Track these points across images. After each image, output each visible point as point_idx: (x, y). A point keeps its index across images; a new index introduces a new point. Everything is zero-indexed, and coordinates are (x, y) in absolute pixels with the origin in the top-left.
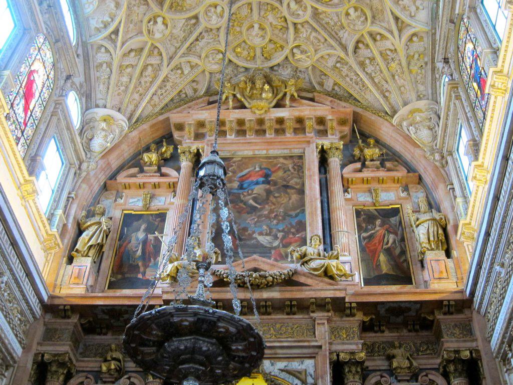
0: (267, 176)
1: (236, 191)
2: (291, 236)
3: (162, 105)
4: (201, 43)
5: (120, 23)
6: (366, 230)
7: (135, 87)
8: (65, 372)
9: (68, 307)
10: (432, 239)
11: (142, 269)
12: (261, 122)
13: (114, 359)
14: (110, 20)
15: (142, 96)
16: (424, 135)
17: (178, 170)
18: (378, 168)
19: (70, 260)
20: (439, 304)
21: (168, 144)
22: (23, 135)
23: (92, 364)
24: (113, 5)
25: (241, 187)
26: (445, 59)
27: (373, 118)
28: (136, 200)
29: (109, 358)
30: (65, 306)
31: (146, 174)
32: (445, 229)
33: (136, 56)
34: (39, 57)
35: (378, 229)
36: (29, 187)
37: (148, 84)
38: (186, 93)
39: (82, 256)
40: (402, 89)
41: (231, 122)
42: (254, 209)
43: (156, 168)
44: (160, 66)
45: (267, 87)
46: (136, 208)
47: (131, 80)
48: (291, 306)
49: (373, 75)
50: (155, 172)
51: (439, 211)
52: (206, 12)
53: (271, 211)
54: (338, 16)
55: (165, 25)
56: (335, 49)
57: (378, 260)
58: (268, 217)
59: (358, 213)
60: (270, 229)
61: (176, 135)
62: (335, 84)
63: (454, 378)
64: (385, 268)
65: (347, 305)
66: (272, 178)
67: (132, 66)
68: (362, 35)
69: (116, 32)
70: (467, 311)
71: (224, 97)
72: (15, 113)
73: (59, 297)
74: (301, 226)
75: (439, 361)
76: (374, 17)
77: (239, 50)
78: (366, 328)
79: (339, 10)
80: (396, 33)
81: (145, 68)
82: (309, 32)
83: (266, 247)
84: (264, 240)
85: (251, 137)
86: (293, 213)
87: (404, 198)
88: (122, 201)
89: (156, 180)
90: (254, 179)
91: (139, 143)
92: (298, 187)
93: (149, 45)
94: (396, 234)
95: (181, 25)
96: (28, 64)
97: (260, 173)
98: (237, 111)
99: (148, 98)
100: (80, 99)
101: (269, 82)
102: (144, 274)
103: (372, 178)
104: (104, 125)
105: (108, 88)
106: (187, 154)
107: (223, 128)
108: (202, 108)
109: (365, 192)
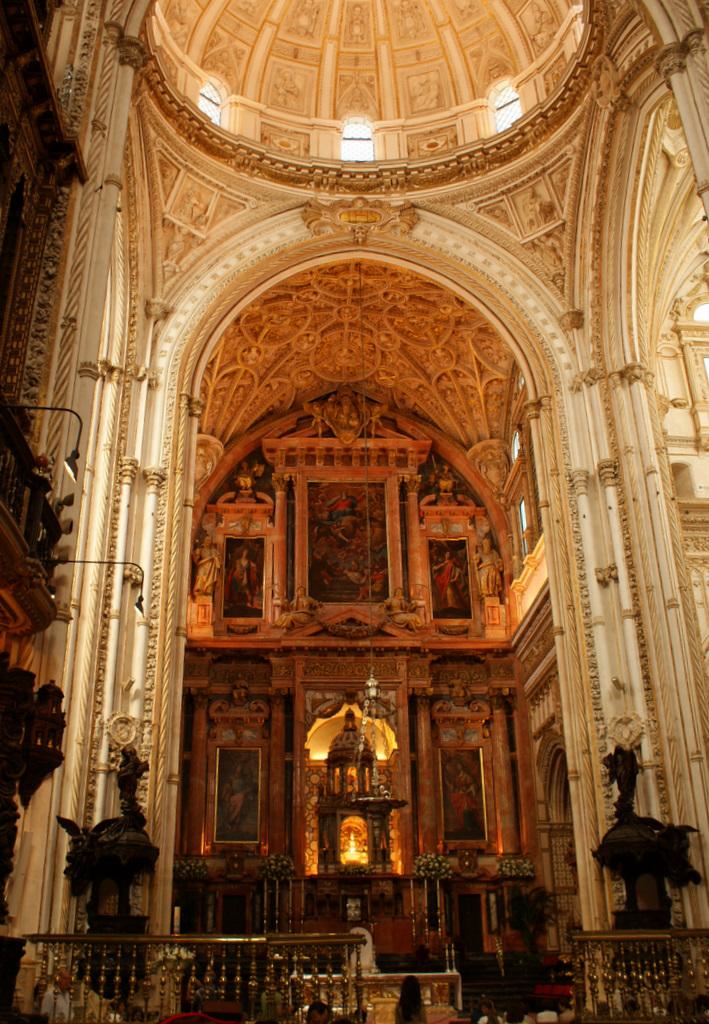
0: (352, 506)
1: (325, 522)
2: (375, 573)
3: (252, 422)
6: (437, 564)
10: (490, 585)
11: (250, 598)
12: (347, 450)
13: (242, 687)
15: (234, 415)
16: (493, 475)
17: (271, 493)
18: (450, 502)
20: (490, 651)
21: (259, 463)
23: (222, 689)
25: (330, 518)
28: (234, 524)
29: (238, 686)
31: (244, 500)
32: (501, 573)
35: (448, 563)
42: (342, 544)
43: (250, 491)
45: (354, 415)
46: (235, 533)
48: (380, 652)
50: (250, 496)
53: (358, 546)
55: (259, 352)
56: (420, 378)
57: (446, 595)
58: (355, 551)
59: (431, 544)
60: (358, 564)
61: (267, 456)
62: (415, 404)
63: (497, 709)
64: (451, 603)
65: (422, 651)
66: (357, 509)
67: (225, 389)
70: (511, 656)
71: (313, 423)
73: (196, 641)
74: (383, 563)
75: (486, 689)
76: (458, 356)
78: (433, 663)
79: (428, 348)
81: (239, 387)
83: (354, 584)
84: (353, 576)
85: (338, 465)
86: (377, 548)
87: (470, 531)
88: (222, 525)
90: (341, 509)
92: (380, 519)
93: (243, 371)
94: (461, 567)
95: (273, 351)
97: (347, 502)
99: (240, 416)
101: (355, 404)
102: (252, 603)
103: (446, 512)
107: (312, 453)
109: (437, 523)
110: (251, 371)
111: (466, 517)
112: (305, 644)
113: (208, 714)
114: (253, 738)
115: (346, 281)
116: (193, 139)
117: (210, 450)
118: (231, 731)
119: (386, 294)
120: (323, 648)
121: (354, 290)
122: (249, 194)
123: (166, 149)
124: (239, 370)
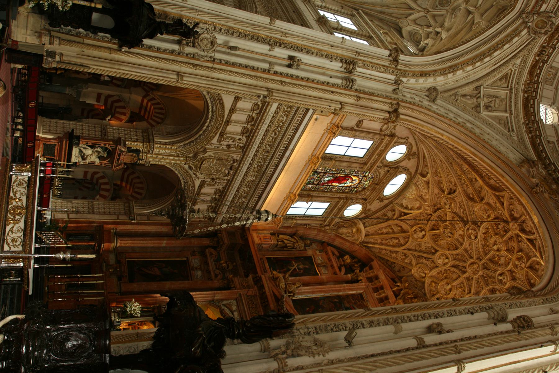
1: (343, 306)
3: (382, 256)
4: (424, 261)
5: (411, 213)
7: (384, 239)
8: (215, 245)
9: (246, 237)
13: (228, 265)
14: (410, 208)
15: (381, 244)
19: (273, 234)
22: (317, 185)
24: (417, 205)
30: (246, 235)
33: (399, 230)
34: (360, 177)
36: (293, 197)
37: (389, 244)
38: (395, 266)
39: (277, 239)
41: (384, 292)
44: (402, 245)
47: (386, 234)
52: (442, 255)
61: (367, 268)
69: (406, 214)
71: (397, 284)
72: (323, 176)
77: (433, 284)
88: (318, 253)
89: (335, 265)
91: (354, 251)
95: (428, 245)
96: (352, 173)
98: (392, 293)
99: (381, 247)
100: (361, 213)
104: (354, 230)
105: (376, 225)
106: (356, 275)
108: (386, 275)
110: (411, 238)
112: (267, 289)
113: (207, 247)
114: (198, 275)
115: (494, 244)
116: (526, 95)
117: (356, 236)
118: (199, 264)
119: (501, 275)
120: (268, 301)
121: (491, 260)
122: (517, 131)
123: (514, 74)
124: (408, 232)
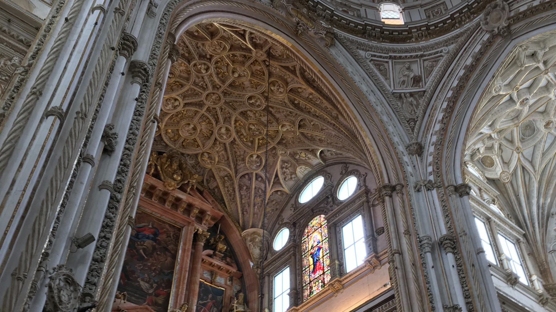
6: (202, 300)
16: (256, 252)
26: (294, 223)
27: (232, 224)
40: (256, 215)
49: (243, 197)
51: (248, 307)
54: (245, 152)
56: (231, 169)
62: (217, 187)
68: (252, 173)
79: (247, 150)
80: (272, 184)
82: (221, 149)
92: (173, 252)
109: (208, 271)
111: (229, 275)
